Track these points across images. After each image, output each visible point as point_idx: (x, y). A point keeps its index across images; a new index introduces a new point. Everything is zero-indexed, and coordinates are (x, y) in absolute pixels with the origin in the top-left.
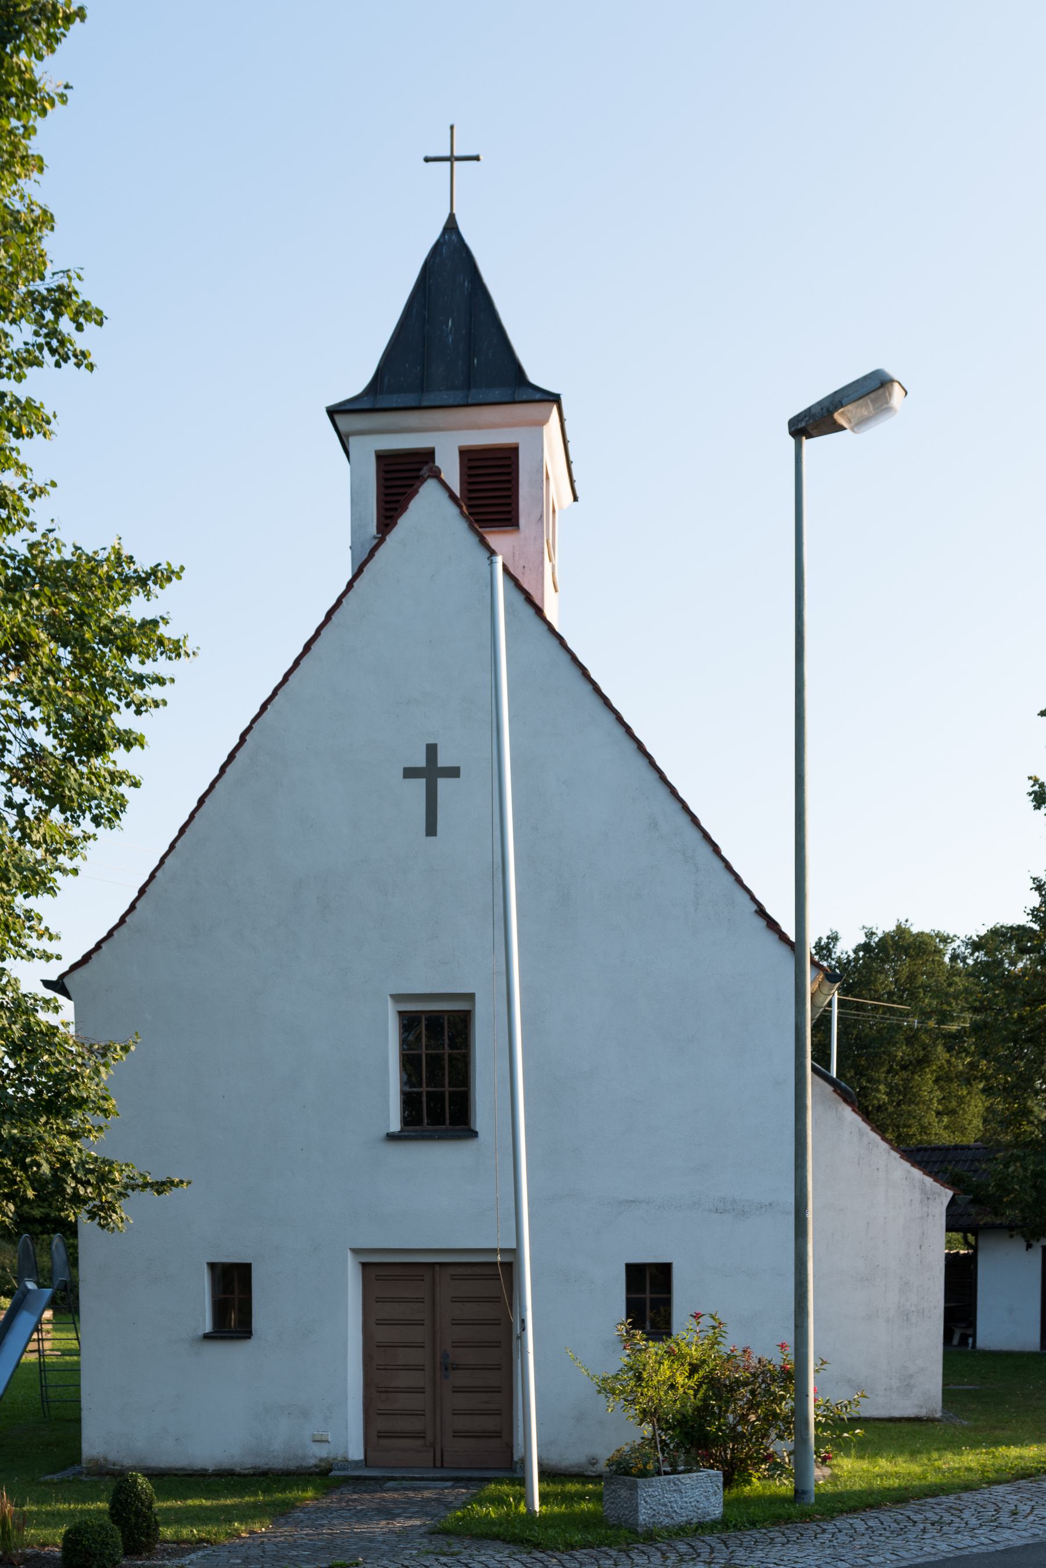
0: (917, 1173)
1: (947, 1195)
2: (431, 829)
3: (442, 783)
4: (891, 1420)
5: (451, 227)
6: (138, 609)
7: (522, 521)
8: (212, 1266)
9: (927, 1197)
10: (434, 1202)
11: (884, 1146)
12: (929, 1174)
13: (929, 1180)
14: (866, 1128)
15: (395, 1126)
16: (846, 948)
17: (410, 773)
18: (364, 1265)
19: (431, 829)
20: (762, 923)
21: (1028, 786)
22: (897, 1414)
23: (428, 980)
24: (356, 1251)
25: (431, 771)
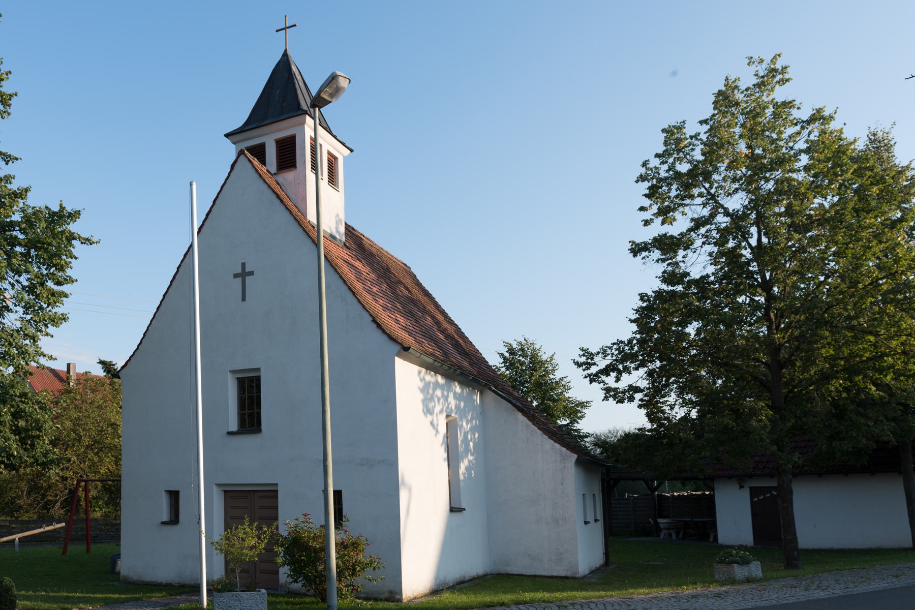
0: (557, 446)
1: (576, 456)
2: (244, 299)
3: (248, 279)
4: (552, 577)
5: (285, 54)
6: (73, 227)
7: (298, 165)
8: (167, 491)
9: (564, 458)
10: (252, 462)
11: (539, 432)
12: (563, 445)
13: (564, 449)
14: (530, 424)
15: (234, 427)
16: (628, 331)
17: (236, 276)
18: (225, 491)
19: (244, 299)
20: (375, 326)
21: (629, 246)
22: (555, 574)
23: (242, 364)
24: (219, 485)
25: (244, 274)
